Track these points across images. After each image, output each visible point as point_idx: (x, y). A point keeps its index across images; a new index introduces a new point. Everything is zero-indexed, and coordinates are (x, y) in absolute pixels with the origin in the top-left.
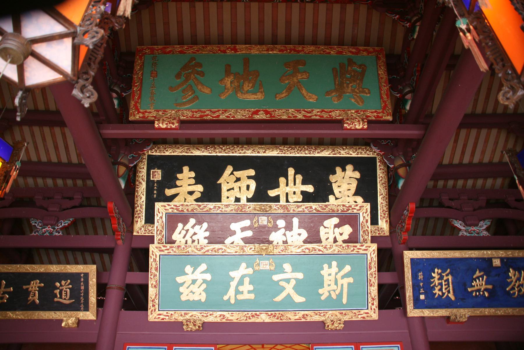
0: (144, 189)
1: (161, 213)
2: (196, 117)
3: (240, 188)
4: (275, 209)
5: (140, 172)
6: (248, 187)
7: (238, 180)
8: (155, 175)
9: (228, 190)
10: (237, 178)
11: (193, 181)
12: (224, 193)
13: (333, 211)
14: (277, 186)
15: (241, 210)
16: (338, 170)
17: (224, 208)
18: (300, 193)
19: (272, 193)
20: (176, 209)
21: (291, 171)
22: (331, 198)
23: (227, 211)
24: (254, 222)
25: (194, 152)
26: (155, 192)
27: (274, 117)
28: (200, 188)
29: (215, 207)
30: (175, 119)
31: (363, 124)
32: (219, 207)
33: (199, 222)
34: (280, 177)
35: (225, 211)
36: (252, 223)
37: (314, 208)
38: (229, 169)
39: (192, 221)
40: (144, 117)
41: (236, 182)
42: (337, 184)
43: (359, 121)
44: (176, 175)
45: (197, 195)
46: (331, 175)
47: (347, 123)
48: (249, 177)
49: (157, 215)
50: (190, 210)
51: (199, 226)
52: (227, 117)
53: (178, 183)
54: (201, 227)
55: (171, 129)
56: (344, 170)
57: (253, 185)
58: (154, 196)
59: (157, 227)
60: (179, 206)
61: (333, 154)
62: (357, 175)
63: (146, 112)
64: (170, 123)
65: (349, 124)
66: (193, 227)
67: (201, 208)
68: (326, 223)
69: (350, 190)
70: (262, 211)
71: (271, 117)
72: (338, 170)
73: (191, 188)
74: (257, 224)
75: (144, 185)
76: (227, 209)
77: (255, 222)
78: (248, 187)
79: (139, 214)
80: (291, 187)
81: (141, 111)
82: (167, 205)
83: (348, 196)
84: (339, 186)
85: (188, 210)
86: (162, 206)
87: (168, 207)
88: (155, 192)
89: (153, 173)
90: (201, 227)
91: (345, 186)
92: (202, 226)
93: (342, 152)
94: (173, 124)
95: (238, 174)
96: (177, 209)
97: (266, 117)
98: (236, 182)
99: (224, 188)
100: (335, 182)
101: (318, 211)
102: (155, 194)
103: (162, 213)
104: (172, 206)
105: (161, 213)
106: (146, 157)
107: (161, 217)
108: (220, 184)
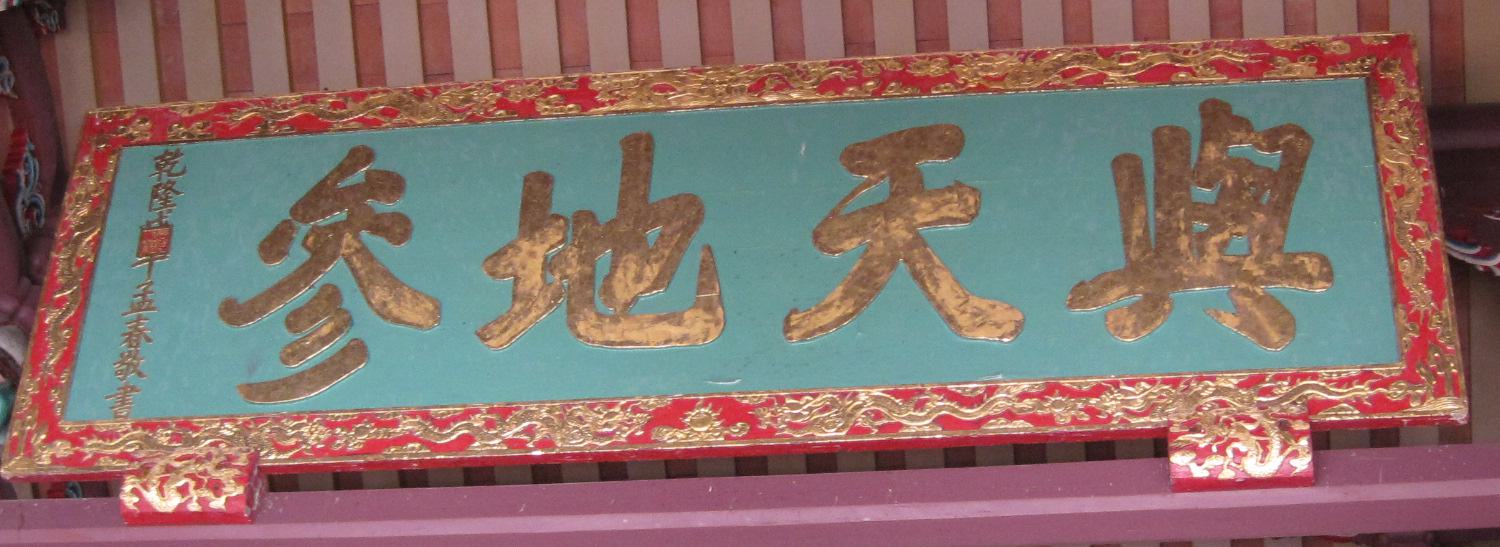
2: (344, 453)
27: (770, 432)
30: (227, 463)
31: (1285, 446)
40: (74, 460)
43: (1259, 432)
47: (1192, 448)
52: (511, 443)
55: (206, 517)
63: (89, 432)
64: (198, 486)
65: (1205, 453)
71: (755, 433)
81: (67, 427)
94: (216, 487)
97: (728, 438)
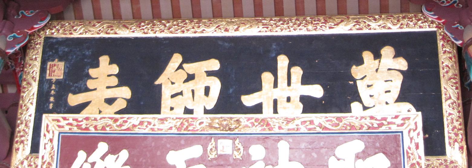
0: (33, 94)
1: (51, 132)
3: (193, 91)
4: (247, 126)
5: (30, 65)
6: (207, 91)
7: (191, 77)
8: (54, 71)
9: (173, 96)
10: (188, 74)
11: (115, 81)
12: (166, 101)
13: (352, 127)
14: (258, 88)
15: (187, 127)
16: (367, 56)
17: (156, 123)
18: (299, 99)
19: (248, 100)
20: (77, 126)
21: (283, 61)
22: (355, 106)
23: (162, 130)
24: (209, 149)
25: (117, 31)
26: (52, 99)
28: (126, 92)
29: (141, 123)
32: (149, 123)
33: (114, 150)
34: (262, 72)
35: (158, 129)
36: (205, 150)
37: (316, 122)
38: (177, 59)
39: (103, 147)
41: (186, 81)
42: (367, 81)
44: (88, 70)
45: (121, 104)
46: (354, 67)
48: (210, 74)
49: (45, 135)
50: (99, 127)
51: (113, 156)
53: (90, 84)
54: (117, 158)
56: (377, 56)
57: (216, 85)
58: (48, 106)
59: (43, 157)
60: (82, 121)
61: (358, 29)
62: (402, 64)
66: (103, 158)
67: (118, 123)
68: (340, 151)
69: (389, 91)
70: (223, 130)
72: (367, 56)
73: (110, 93)
74: (215, 153)
75: (34, 88)
76: (161, 126)
77: (211, 149)
78: (207, 91)
79: (22, 136)
80: (283, 90)
82: (61, 119)
83: (387, 103)
84: (368, 86)
85: (96, 128)
86: (53, 120)
87: (63, 123)
88: (52, 99)
89: (50, 68)
90: (117, 158)
91: (380, 86)
92: (118, 156)
93: (373, 24)
95: (190, 68)
96: (79, 126)
98: (186, 81)
99: (166, 92)
100: (362, 79)
101: (325, 128)
102: (52, 102)
103: (53, 132)
104: (71, 121)
105: (51, 132)
106: (41, 40)
107: (51, 140)
108: (160, 86)
